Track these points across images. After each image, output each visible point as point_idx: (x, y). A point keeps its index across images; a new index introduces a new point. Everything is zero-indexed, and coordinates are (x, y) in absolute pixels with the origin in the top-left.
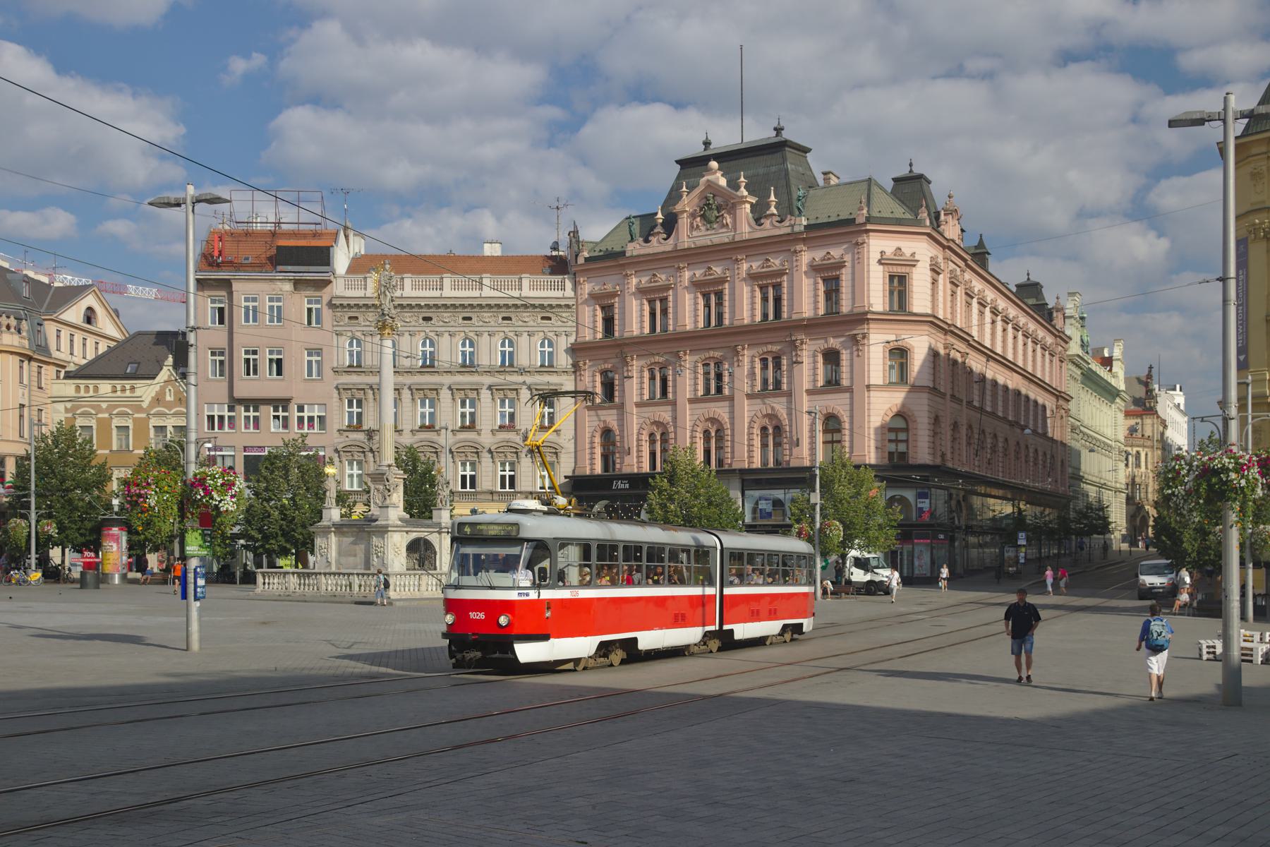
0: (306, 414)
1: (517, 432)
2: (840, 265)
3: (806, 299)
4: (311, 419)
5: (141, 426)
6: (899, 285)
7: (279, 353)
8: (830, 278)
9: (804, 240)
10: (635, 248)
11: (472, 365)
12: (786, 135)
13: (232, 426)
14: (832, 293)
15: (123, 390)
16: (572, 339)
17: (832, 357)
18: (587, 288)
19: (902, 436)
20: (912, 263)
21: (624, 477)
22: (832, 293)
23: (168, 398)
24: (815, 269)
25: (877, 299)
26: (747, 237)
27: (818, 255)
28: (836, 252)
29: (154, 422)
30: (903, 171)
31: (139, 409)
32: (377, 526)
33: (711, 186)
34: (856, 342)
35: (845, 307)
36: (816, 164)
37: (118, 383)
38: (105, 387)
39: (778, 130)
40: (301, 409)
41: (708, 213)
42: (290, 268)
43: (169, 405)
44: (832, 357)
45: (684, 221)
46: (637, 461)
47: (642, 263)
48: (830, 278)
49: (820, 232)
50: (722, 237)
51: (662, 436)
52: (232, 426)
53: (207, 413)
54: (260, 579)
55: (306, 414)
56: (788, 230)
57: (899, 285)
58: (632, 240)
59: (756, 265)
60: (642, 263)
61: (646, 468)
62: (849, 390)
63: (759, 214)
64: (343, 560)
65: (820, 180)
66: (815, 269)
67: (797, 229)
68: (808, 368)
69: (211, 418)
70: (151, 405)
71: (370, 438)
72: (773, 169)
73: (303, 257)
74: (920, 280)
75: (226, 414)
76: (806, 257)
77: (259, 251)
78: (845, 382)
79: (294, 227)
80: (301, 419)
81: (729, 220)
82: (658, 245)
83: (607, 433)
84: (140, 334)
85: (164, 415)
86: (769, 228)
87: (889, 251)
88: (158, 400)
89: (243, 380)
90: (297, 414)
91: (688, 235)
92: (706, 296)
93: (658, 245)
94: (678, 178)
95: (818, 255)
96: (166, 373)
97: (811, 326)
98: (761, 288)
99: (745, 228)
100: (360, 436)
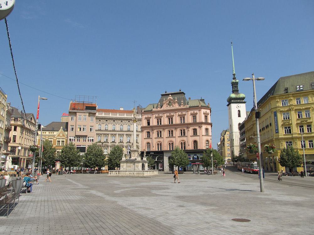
0: (90, 139)
1: (131, 143)
2: (197, 114)
3: (189, 119)
4: (90, 140)
6: (206, 117)
7: (80, 126)
8: (194, 116)
9: (189, 109)
11: (130, 130)
12: (182, 91)
13: (74, 141)
15: (51, 133)
16: (141, 126)
17: (195, 131)
18: (145, 116)
19: (208, 144)
21: (152, 152)
23: (61, 135)
24: (191, 114)
25: (203, 120)
26: (178, 108)
27: (192, 112)
28: (196, 112)
29: (57, 140)
32: (137, 161)
33: (170, 99)
34: (200, 127)
35: (198, 121)
36: (187, 96)
38: (47, 133)
39: (180, 91)
40: (89, 138)
41: (170, 104)
42: (88, 110)
43: (61, 137)
44: (195, 130)
46: (154, 148)
47: (156, 112)
48: (194, 116)
49: (191, 108)
51: (160, 145)
52: (74, 141)
53: (69, 138)
54: (109, 172)
55: (90, 139)
56: (186, 107)
57: (206, 117)
58: (154, 108)
59: (180, 113)
60: (156, 112)
61: (157, 150)
62: (199, 136)
64: (127, 168)
66: (191, 114)
67: (187, 107)
68: (190, 132)
69: (70, 139)
70: (57, 137)
71: (102, 144)
72: (181, 97)
73: (91, 109)
75: (73, 138)
76: (190, 112)
78: (198, 134)
79: (87, 103)
80: (88, 140)
81: (174, 105)
82: (159, 109)
83: (148, 143)
84: (53, 122)
85: (60, 139)
86: (182, 107)
87: (205, 112)
88: (59, 136)
89: (70, 132)
90: (88, 139)
91: (165, 107)
92: (169, 119)
94: (161, 97)
95: (192, 112)
96: (60, 131)
97: (190, 124)
98: (180, 117)
99: (176, 106)
100: (101, 144)
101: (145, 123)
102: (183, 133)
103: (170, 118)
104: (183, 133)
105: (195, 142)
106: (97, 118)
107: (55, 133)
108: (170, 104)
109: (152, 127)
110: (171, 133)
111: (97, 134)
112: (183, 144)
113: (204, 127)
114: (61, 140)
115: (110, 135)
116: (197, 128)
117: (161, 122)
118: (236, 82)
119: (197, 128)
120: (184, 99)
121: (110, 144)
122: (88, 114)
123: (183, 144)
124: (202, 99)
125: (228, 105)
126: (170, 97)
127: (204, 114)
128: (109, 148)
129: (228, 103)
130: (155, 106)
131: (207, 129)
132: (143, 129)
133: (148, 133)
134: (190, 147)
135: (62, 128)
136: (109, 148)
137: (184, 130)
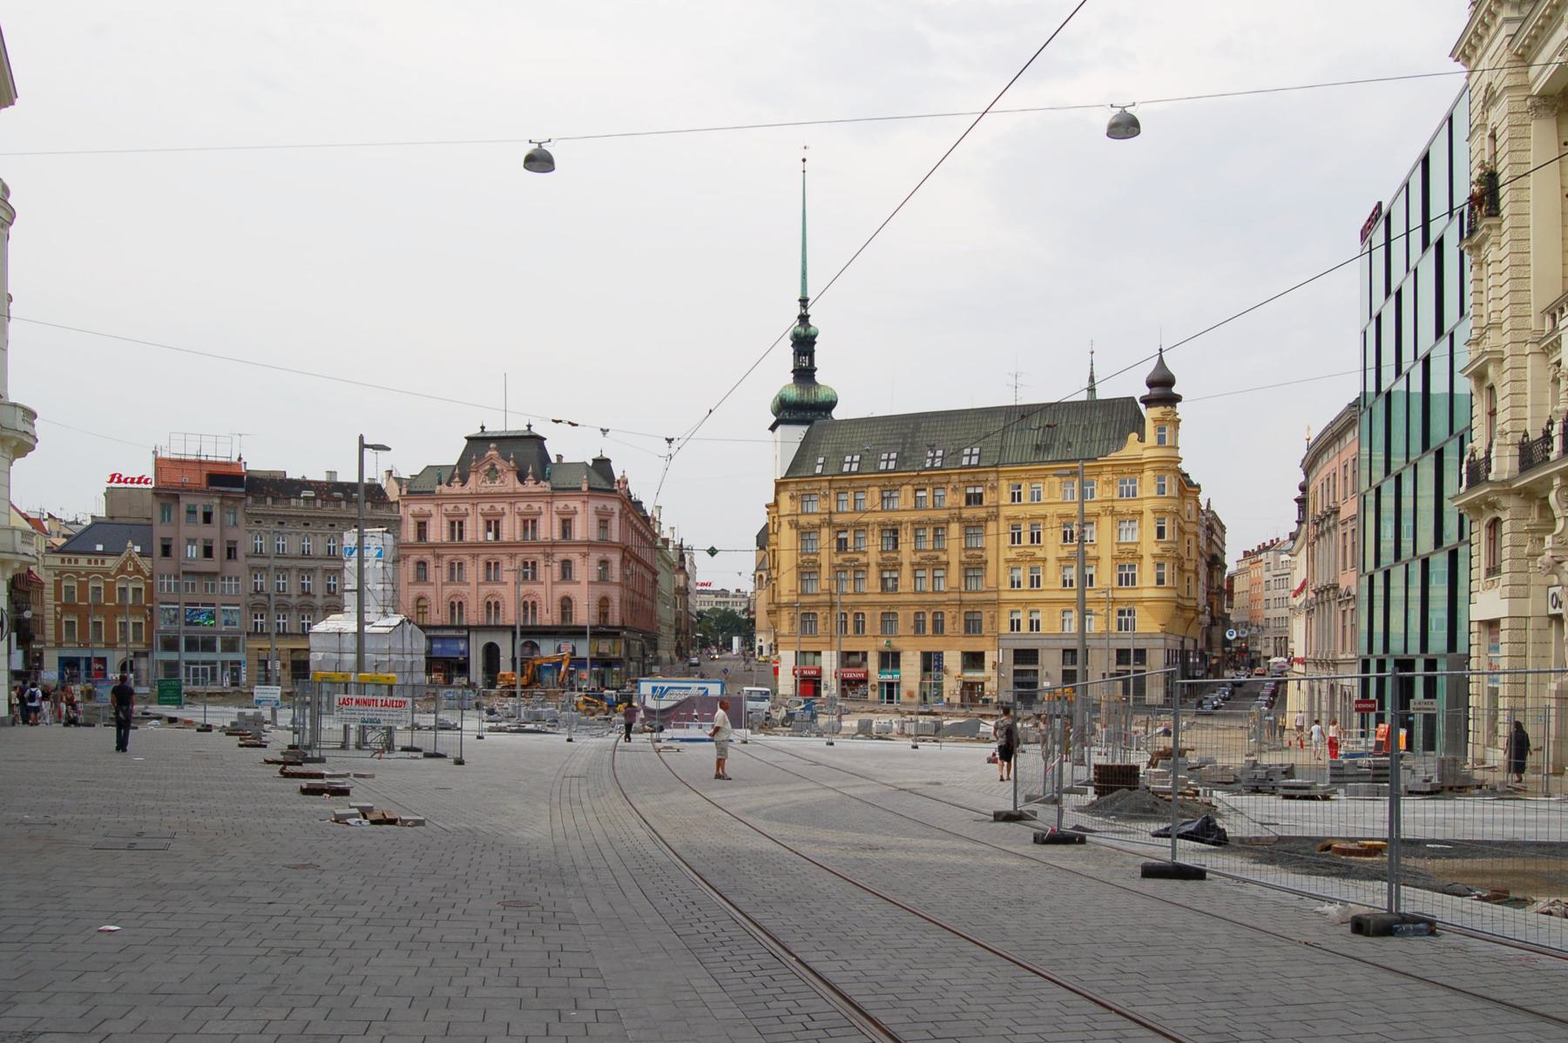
2: (575, 513)
5: (110, 587)
10: (445, 489)
12: (536, 430)
14: (566, 526)
17: (566, 566)
20: (611, 514)
22: (566, 526)
29: (118, 585)
30: (597, 455)
31: (107, 575)
37: (93, 558)
43: (130, 574)
45: (472, 478)
50: (497, 487)
57: (604, 524)
63: (522, 478)
65: (554, 460)
70: (117, 574)
74: (615, 523)
77: (199, 479)
88: (122, 570)
93: (456, 488)
101: (410, 534)
102: (529, 572)
103: (493, 524)
104: (529, 572)
105: (566, 604)
106: (250, 516)
107: (111, 563)
108: (493, 473)
109: (433, 547)
110: (492, 567)
111: (252, 568)
112: (529, 607)
113: (595, 556)
114: (131, 586)
115: (294, 573)
116: (575, 557)
117: (461, 532)
118: (806, 337)
119: (575, 557)
120: (545, 458)
121: (294, 601)
122: (217, 501)
123: (529, 607)
124: (605, 456)
125: (773, 428)
126: (492, 452)
127: (598, 513)
128: (294, 613)
129: (774, 419)
130: (445, 479)
131: (604, 563)
132: (402, 552)
133: (421, 565)
134: (548, 616)
135: (130, 544)
136: (294, 613)
137: (534, 564)
